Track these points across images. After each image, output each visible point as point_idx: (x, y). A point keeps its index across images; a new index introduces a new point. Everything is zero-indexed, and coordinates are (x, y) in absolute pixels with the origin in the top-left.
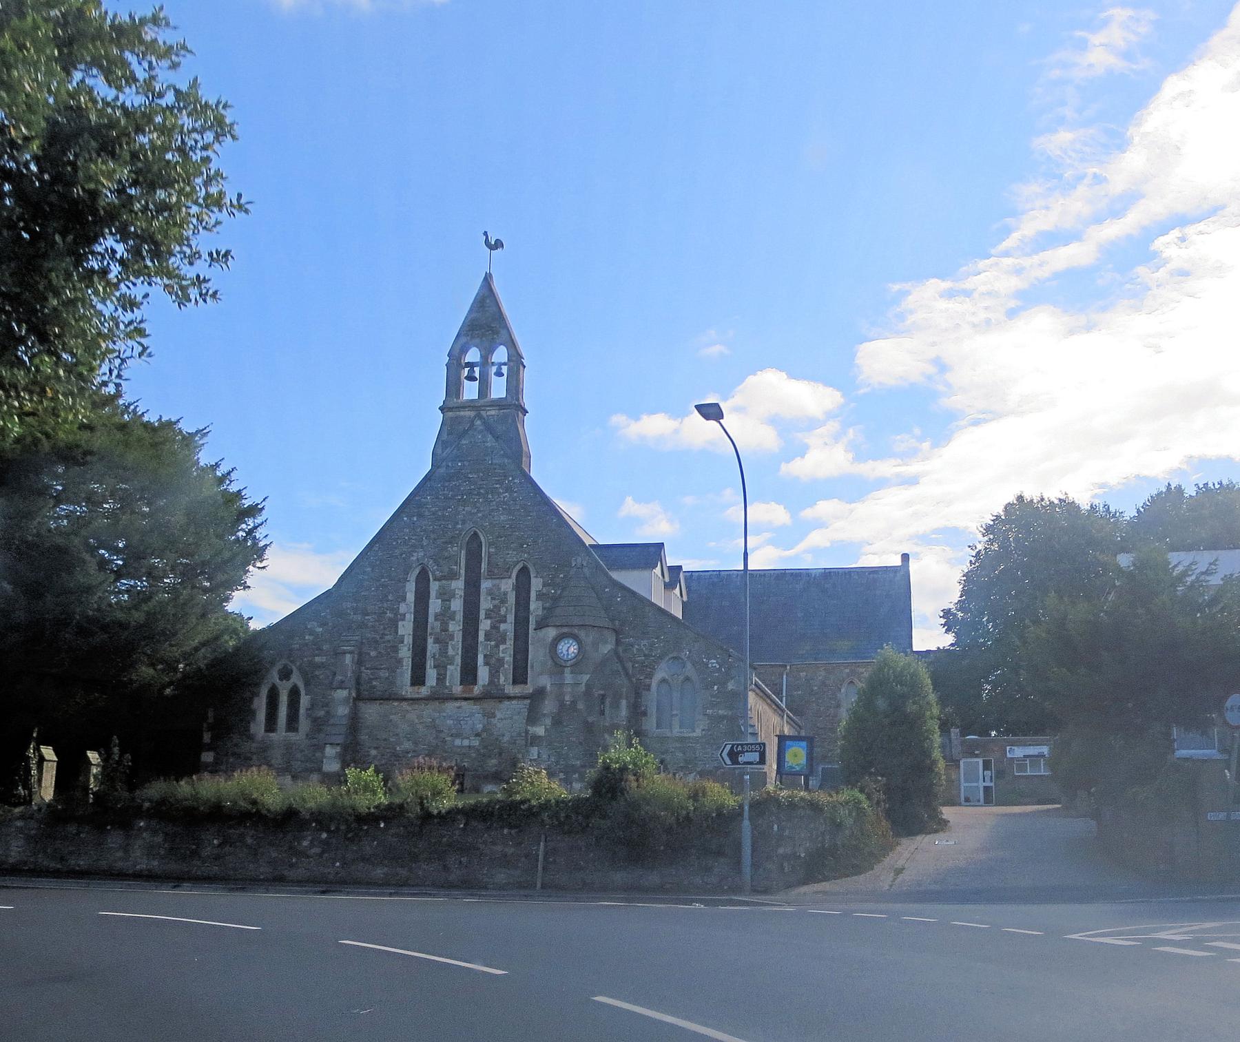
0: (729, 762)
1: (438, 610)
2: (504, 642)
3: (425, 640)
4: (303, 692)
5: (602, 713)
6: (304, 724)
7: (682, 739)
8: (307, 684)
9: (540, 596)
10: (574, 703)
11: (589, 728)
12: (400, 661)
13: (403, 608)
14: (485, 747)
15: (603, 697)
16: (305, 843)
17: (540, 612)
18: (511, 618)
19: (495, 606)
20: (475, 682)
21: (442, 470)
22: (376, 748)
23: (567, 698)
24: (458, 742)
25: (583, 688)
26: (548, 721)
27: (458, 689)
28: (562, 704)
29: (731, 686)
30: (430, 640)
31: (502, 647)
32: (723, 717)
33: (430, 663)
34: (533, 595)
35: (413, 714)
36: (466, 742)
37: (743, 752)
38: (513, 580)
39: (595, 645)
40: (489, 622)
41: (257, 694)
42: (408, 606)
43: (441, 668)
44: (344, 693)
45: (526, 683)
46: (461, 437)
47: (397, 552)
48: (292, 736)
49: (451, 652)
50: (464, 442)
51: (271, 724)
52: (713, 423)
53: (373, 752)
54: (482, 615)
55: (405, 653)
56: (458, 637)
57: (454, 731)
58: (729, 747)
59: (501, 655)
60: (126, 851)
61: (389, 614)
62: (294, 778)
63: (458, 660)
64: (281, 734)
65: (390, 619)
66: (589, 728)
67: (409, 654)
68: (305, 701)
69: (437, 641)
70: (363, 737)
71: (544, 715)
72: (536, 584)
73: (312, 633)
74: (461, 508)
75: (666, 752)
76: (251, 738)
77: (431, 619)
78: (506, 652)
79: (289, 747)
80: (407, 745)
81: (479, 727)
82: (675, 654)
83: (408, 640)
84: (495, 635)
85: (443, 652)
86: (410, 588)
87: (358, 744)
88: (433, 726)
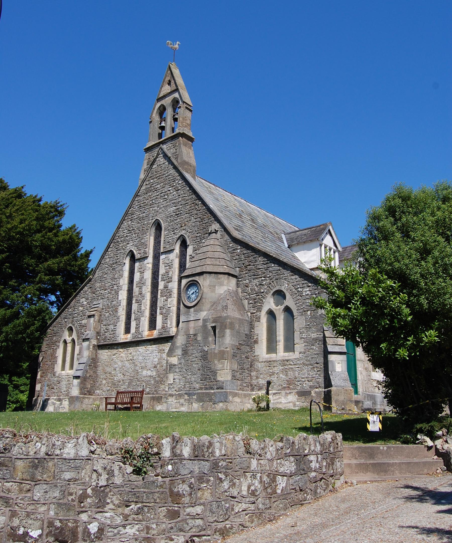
7: (284, 362)
10: (195, 335)
14: (159, 377)
15: (214, 328)
21: (144, 188)
22: (105, 379)
24: (145, 373)
25: (200, 323)
27: (146, 334)
28: (188, 336)
30: (134, 302)
31: (169, 300)
32: (316, 339)
35: (123, 353)
36: (149, 373)
38: (177, 250)
39: (212, 287)
40: (163, 282)
41: (58, 346)
42: (124, 281)
43: (138, 319)
46: (152, 164)
47: (120, 245)
49: (143, 308)
50: (154, 167)
53: (104, 382)
55: (122, 313)
57: (143, 365)
59: (169, 306)
61: (115, 287)
66: (205, 356)
69: (137, 301)
72: (190, 251)
74: (151, 209)
75: (273, 373)
80: (120, 377)
83: (124, 303)
85: (139, 310)
86: (127, 268)
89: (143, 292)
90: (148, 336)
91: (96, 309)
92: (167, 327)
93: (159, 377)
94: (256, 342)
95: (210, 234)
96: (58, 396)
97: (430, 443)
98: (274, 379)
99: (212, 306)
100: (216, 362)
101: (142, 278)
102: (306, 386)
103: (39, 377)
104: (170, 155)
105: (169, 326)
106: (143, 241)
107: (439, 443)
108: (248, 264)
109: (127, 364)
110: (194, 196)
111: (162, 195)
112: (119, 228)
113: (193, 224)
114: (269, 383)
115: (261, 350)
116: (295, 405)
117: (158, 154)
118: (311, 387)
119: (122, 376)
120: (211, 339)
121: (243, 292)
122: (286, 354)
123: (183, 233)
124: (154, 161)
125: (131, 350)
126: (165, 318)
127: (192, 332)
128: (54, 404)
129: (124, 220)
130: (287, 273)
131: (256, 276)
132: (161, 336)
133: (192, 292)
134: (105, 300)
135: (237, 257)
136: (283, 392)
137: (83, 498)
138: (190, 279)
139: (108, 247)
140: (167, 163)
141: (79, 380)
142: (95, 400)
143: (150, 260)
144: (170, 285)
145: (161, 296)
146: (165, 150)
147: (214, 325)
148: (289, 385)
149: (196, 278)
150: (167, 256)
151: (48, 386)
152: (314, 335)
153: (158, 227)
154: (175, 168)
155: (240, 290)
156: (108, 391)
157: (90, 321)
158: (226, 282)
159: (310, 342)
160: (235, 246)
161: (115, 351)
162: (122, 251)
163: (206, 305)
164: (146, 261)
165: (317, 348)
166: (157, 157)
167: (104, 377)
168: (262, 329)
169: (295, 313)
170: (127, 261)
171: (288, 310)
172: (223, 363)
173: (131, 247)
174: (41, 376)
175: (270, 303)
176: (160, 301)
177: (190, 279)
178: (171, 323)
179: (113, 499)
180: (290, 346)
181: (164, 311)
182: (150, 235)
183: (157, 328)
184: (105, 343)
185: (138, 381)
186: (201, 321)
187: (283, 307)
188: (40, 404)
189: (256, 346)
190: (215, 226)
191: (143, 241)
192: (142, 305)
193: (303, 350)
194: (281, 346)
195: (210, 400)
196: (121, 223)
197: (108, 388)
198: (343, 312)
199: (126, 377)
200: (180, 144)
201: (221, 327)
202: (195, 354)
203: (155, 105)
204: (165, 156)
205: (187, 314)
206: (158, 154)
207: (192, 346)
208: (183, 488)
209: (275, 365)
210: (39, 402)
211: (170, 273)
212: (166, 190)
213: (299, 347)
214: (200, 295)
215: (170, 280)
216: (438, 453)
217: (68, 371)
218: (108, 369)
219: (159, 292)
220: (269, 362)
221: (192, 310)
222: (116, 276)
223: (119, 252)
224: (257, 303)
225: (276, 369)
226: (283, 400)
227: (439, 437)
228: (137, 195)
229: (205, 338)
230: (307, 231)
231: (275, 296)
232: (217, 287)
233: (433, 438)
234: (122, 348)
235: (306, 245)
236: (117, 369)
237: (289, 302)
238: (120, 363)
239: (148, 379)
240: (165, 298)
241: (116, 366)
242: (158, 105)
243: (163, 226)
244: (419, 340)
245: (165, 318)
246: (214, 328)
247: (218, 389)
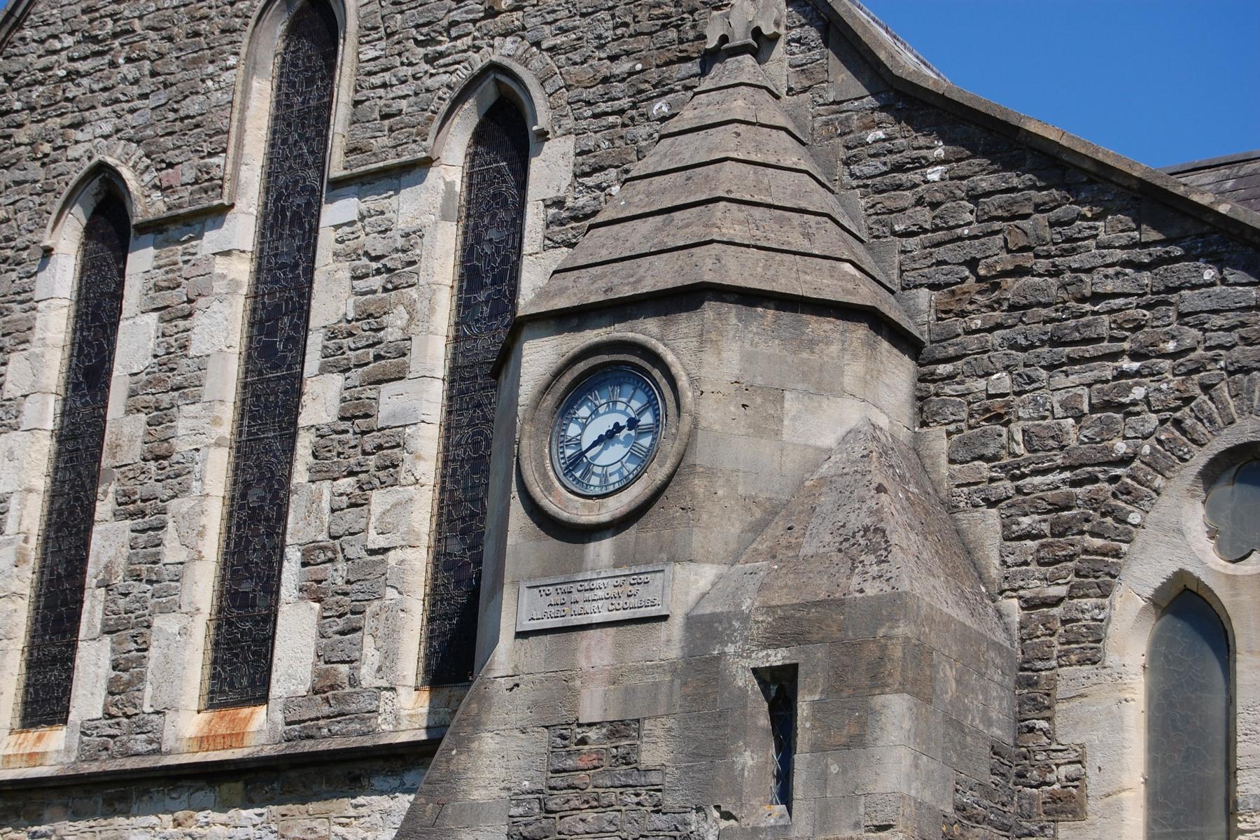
10: (618, 729)
15: (780, 687)
18: (433, 352)
25: (668, 644)
27: (186, 727)
28: (565, 734)
30: (104, 508)
31: (379, 500)
39: (760, 399)
40: (337, 380)
43: (130, 630)
47: (21, 136)
49: (172, 551)
54: (313, 360)
59: (375, 541)
69: (129, 507)
72: (550, 171)
84: (368, 452)
86: (61, 280)
89: (182, 446)
90: (203, 741)
92: (353, 681)
95: (710, 58)
99: (758, 528)
101: (172, 353)
106: (192, 106)
108: (1006, 261)
120: (753, 759)
123: (504, 50)
126: (344, 619)
127: (593, 705)
131: (1067, 349)
132: (307, 746)
135: (924, 216)
138: (592, 336)
143: (242, 228)
144: (390, 402)
145: (317, 475)
147: (777, 658)
149: (646, 331)
150: (372, 202)
155: (939, 442)
158: (853, 371)
160: (908, 140)
162: (35, 171)
163: (718, 520)
164: (211, 240)
170: (67, 239)
176: (309, 511)
177: (592, 336)
178: (389, 658)
181: (337, 574)
182: (252, 69)
183: (278, 689)
186: (675, 629)
191: (192, 106)
192: (170, 536)
201: (838, 679)
205: (564, 580)
207: (597, 804)
211: (395, 325)
214: (671, 450)
215: (390, 365)
219: (304, 444)
221: (602, 550)
224: (1077, 528)
229: (706, 752)
231: (1224, 490)
232: (791, 403)
240: (346, 484)
245: (344, 619)
246: (780, 687)
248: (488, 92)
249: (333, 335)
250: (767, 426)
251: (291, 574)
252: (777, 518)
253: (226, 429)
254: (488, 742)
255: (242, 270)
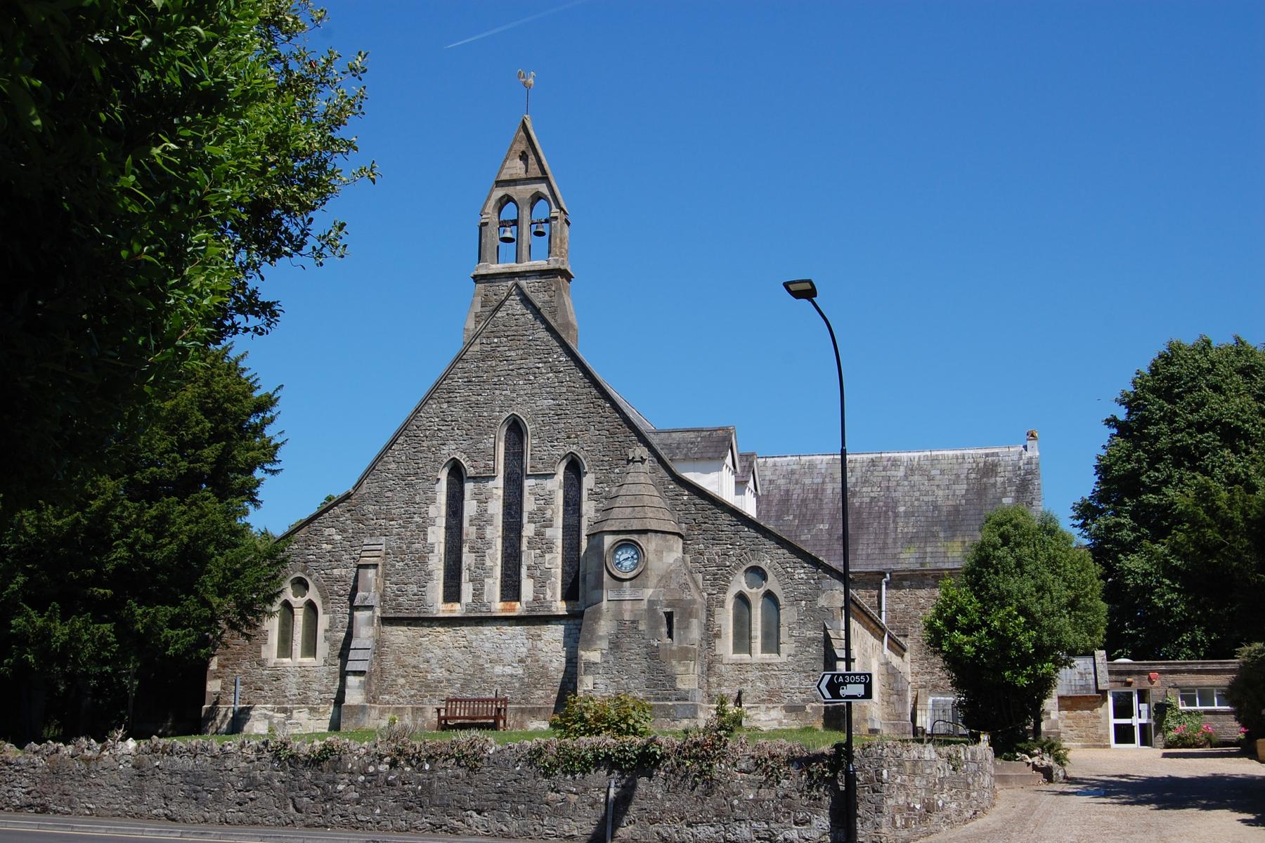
0: (828, 695)
1: (473, 513)
2: (550, 549)
3: (461, 550)
4: (320, 611)
5: (670, 635)
6: (323, 647)
7: (764, 666)
8: (325, 600)
9: (593, 495)
10: (633, 622)
11: (653, 654)
12: (429, 574)
13: (432, 511)
15: (669, 616)
16: (340, 787)
17: (592, 513)
18: (559, 521)
19: (539, 509)
20: (517, 598)
21: (476, 348)
23: (627, 617)
24: (498, 669)
25: (644, 605)
26: (604, 645)
27: (498, 607)
28: (621, 622)
29: (822, 602)
30: (465, 549)
32: (813, 640)
33: (465, 575)
34: (585, 493)
35: (445, 635)
36: (508, 670)
37: (846, 684)
38: (560, 476)
39: (659, 553)
42: (439, 509)
43: (478, 582)
44: (368, 613)
45: (577, 599)
46: (497, 309)
47: (425, 444)
48: (308, 661)
49: (488, 563)
50: (499, 314)
51: (285, 647)
52: (804, 302)
53: (401, 681)
54: (525, 520)
55: (437, 564)
56: (498, 544)
57: (493, 656)
58: (827, 678)
60: (141, 791)
61: (417, 519)
62: (312, 710)
63: (498, 572)
64: (298, 658)
65: (418, 526)
66: (653, 654)
67: (441, 566)
68: (323, 621)
70: (389, 662)
71: (601, 638)
72: (588, 482)
73: (330, 541)
74: (497, 392)
75: (746, 681)
76: (261, 663)
77: (466, 523)
78: (555, 562)
79: (304, 672)
80: (440, 673)
81: (523, 651)
82: (753, 563)
83: (440, 549)
85: (480, 563)
86: (442, 487)
87: (382, 671)
88: (468, 648)
89: (488, 536)
90: (503, 610)
91: (376, 553)
93: (530, 676)
94: (718, 635)
95: (629, 461)
96: (275, 703)
97: (1030, 761)
98: (747, 688)
100: (674, 663)
102: (798, 699)
103: (214, 665)
104: (539, 305)
105: (548, 597)
107: (1036, 760)
108: (702, 520)
109: (456, 654)
110: (594, 392)
111: (522, 371)
112: (418, 410)
113: (594, 438)
114: (740, 693)
115: (725, 646)
116: (780, 723)
117: (509, 294)
118: (804, 700)
119: (446, 674)
120: (664, 630)
121: (694, 561)
122: (767, 656)
123: (574, 448)
124: (502, 303)
125: (465, 630)
126: (541, 584)
127: (627, 617)
128: (266, 716)
129: (431, 398)
130: (770, 544)
131: (716, 540)
133: (625, 556)
134: (393, 538)
136: (763, 706)
137: (935, 784)
138: (623, 537)
139: (394, 441)
140: (530, 316)
141: (362, 679)
142: (382, 712)
143: (500, 481)
145: (529, 548)
146: (527, 291)
148: (771, 697)
149: (635, 537)
150: (538, 481)
151: (243, 684)
152: (810, 634)
153: (516, 429)
154: (550, 329)
155: (688, 559)
156: (412, 696)
157: (365, 575)
159: (805, 643)
160: (679, 489)
161: (426, 630)
162: (430, 455)
163: (653, 580)
164: (491, 484)
165: (816, 651)
166: (506, 299)
167: (401, 671)
168: (726, 619)
169: (782, 601)
170: (443, 475)
171: (769, 595)
172: (688, 666)
173: (450, 451)
174: (219, 665)
175: (739, 583)
176: (528, 557)
177: (623, 537)
178: (554, 594)
179: (946, 786)
180: (772, 643)
183: (523, 599)
184: (401, 615)
185: (484, 682)
186: (645, 602)
187: (762, 591)
188: (226, 715)
189: (717, 641)
190: (640, 451)
193: (793, 652)
194: (757, 644)
195: (667, 716)
196: (425, 402)
197: (413, 692)
198: (966, 639)
199: (454, 676)
200: (559, 289)
202: (634, 650)
203: (492, 190)
204: (526, 301)
205: (619, 590)
206: (509, 294)
208: (970, 780)
209: (749, 668)
210: (222, 713)
211: (548, 514)
212: (531, 365)
213: (787, 647)
215: (549, 524)
216: (1035, 768)
217: (298, 658)
218: (410, 660)
219: (525, 541)
220: (740, 666)
222: (417, 499)
223: (420, 455)
224: (719, 580)
225: (749, 674)
226: (763, 717)
227: (1035, 755)
228: (459, 358)
229: (654, 627)
230: (692, 435)
231: (750, 575)
233: (1031, 756)
234: (442, 626)
235: (701, 464)
236: (433, 661)
237: (772, 584)
238: (437, 651)
239: (508, 679)
241: (430, 655)
242: (499, 193)
243: (530, 428)
244: (1035, 669)
245: (541, 584)
246: (669, 616)
247: (678, 700)
248: (569, 458)
249: (530, 513)
250: (660, 559)
251: (524, 571)
252: (665, 578)
253: (500, 533)
254: (602, 622)
255: (501, 492)
